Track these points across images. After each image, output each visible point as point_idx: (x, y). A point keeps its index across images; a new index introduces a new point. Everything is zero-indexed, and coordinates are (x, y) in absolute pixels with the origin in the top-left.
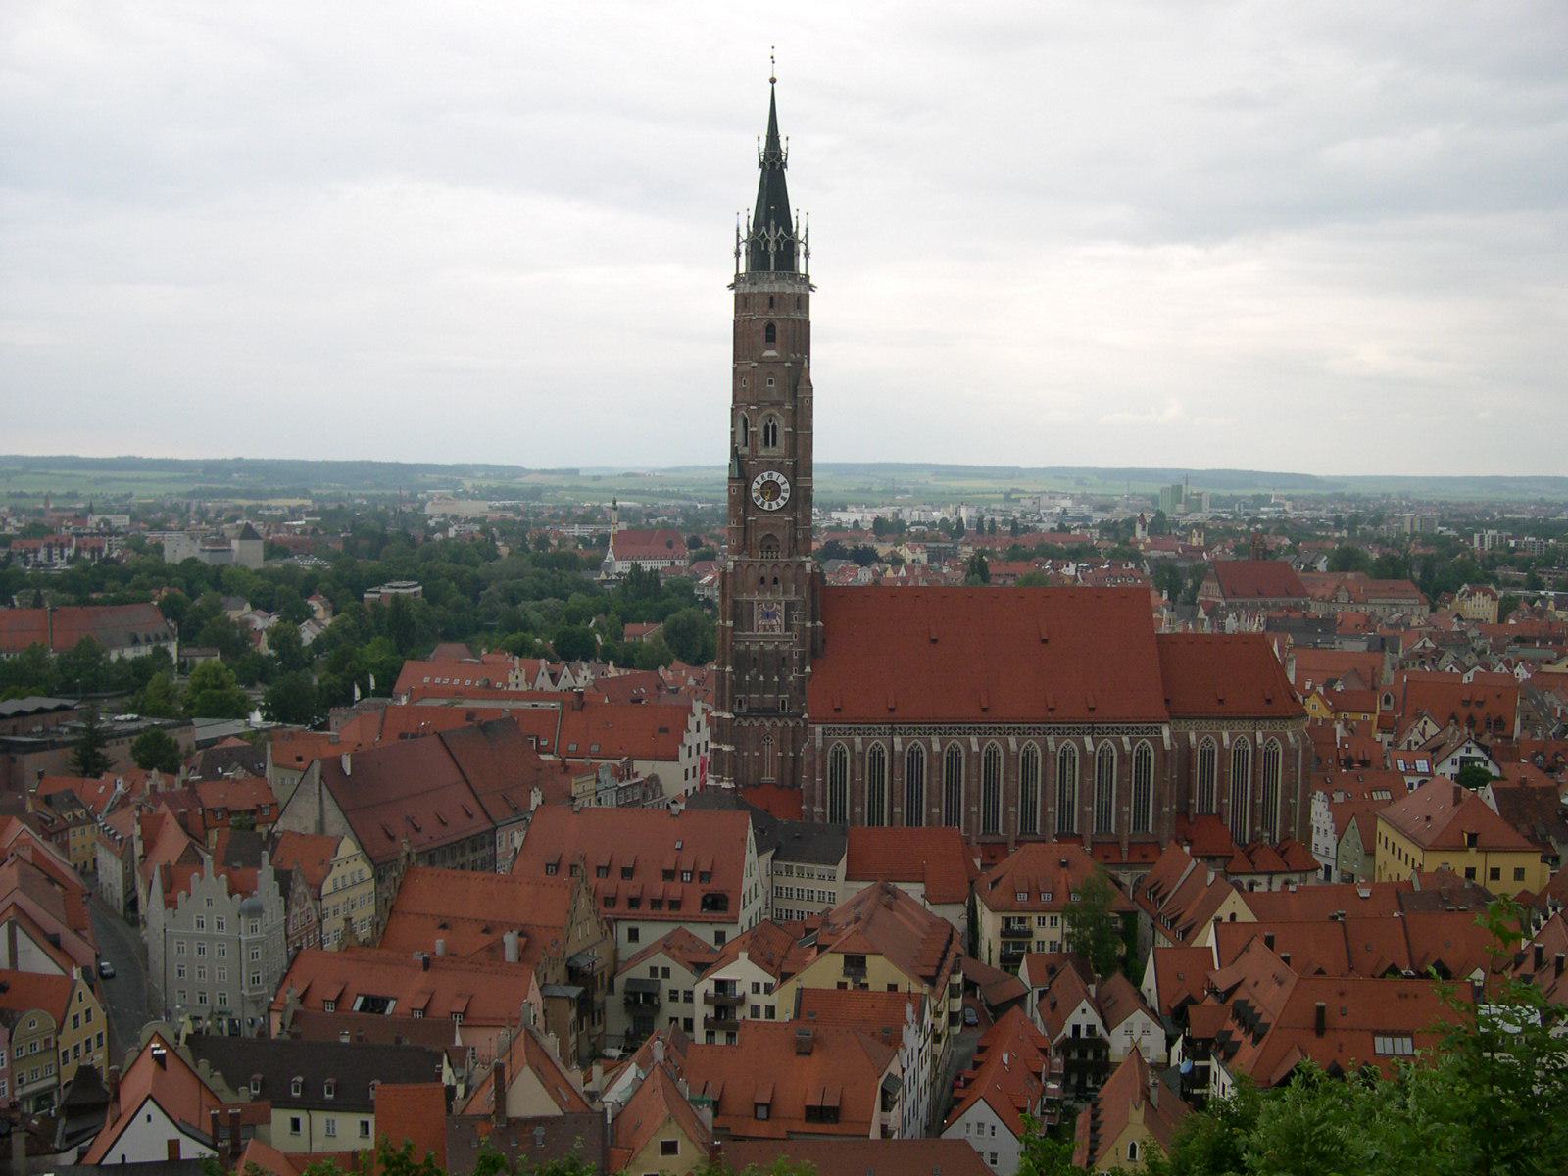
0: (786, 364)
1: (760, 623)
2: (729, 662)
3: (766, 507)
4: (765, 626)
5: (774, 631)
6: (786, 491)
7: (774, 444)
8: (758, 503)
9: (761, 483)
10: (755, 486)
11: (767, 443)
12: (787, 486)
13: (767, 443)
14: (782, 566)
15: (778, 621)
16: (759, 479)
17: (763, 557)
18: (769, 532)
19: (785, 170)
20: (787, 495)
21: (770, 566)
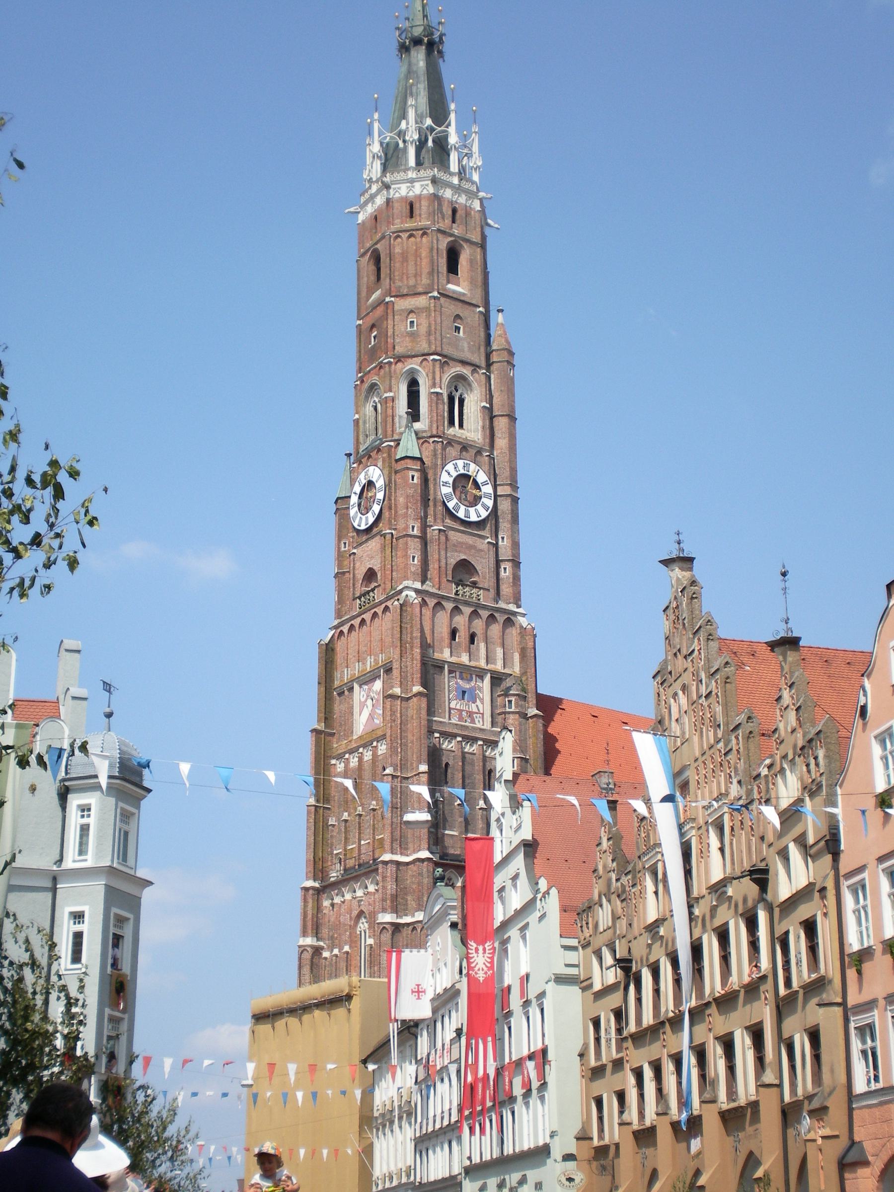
0: (478, 310)
1: (453, 705)
2: (425, 756)
3: (461, 514)
4: (461, 711)
5: (473, 721)
6: (487, 496)
7: (461, 426)
8: (451, 505)
9: (454, 474)
10: (445, 477)
11: (451, 423)
12: (488, 489)
13: (451, 423)
14: (485, 614)
15: (483, 705)
16: (450, 467)
17: (457, 594)
18: (464, 557)
19: (441, 61)
20: (490, 503)
21: (467, 610)
